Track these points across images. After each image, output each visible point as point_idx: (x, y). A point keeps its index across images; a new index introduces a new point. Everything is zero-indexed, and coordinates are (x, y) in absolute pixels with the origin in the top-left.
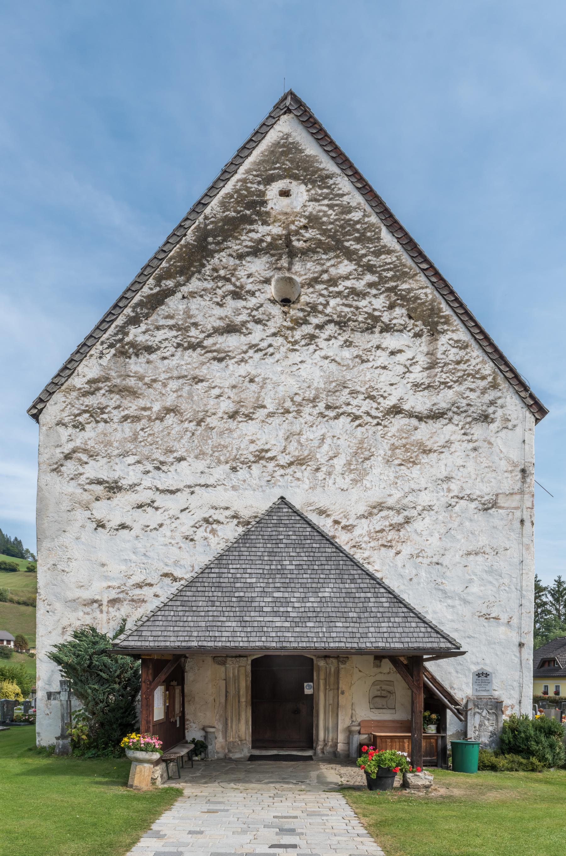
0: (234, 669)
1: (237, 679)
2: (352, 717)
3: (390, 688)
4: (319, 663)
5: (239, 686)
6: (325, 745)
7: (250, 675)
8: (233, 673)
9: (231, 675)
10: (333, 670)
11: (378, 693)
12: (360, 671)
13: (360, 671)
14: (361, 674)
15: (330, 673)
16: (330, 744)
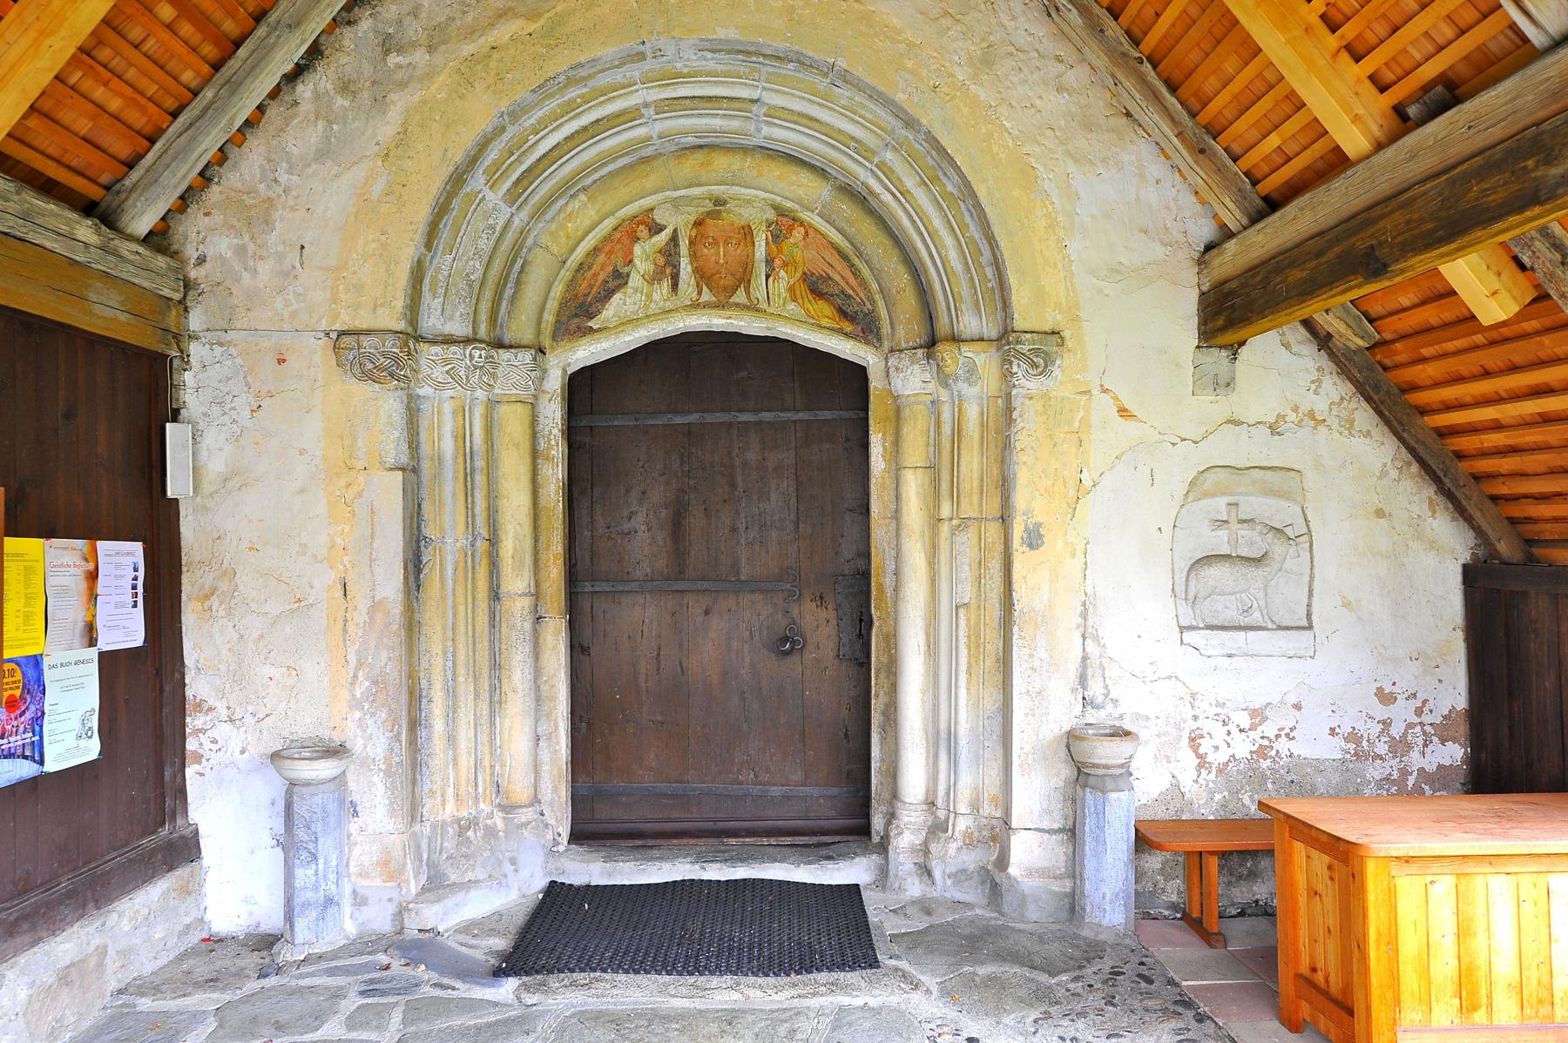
0: (462, 412)
1: (478, 470)
2: (1083, 680)
3: (1282, 512)
4: (898, 383)
6: (938, 829)
7: (557, 449)
8: (461, 437)
9: (448, 446)
10: (972, 412)
11: (1220, 542)
12: (1123, 412)
13: (1123, 412)
14: (1130, 426)
15: (958, 432)
16: (962, 824)
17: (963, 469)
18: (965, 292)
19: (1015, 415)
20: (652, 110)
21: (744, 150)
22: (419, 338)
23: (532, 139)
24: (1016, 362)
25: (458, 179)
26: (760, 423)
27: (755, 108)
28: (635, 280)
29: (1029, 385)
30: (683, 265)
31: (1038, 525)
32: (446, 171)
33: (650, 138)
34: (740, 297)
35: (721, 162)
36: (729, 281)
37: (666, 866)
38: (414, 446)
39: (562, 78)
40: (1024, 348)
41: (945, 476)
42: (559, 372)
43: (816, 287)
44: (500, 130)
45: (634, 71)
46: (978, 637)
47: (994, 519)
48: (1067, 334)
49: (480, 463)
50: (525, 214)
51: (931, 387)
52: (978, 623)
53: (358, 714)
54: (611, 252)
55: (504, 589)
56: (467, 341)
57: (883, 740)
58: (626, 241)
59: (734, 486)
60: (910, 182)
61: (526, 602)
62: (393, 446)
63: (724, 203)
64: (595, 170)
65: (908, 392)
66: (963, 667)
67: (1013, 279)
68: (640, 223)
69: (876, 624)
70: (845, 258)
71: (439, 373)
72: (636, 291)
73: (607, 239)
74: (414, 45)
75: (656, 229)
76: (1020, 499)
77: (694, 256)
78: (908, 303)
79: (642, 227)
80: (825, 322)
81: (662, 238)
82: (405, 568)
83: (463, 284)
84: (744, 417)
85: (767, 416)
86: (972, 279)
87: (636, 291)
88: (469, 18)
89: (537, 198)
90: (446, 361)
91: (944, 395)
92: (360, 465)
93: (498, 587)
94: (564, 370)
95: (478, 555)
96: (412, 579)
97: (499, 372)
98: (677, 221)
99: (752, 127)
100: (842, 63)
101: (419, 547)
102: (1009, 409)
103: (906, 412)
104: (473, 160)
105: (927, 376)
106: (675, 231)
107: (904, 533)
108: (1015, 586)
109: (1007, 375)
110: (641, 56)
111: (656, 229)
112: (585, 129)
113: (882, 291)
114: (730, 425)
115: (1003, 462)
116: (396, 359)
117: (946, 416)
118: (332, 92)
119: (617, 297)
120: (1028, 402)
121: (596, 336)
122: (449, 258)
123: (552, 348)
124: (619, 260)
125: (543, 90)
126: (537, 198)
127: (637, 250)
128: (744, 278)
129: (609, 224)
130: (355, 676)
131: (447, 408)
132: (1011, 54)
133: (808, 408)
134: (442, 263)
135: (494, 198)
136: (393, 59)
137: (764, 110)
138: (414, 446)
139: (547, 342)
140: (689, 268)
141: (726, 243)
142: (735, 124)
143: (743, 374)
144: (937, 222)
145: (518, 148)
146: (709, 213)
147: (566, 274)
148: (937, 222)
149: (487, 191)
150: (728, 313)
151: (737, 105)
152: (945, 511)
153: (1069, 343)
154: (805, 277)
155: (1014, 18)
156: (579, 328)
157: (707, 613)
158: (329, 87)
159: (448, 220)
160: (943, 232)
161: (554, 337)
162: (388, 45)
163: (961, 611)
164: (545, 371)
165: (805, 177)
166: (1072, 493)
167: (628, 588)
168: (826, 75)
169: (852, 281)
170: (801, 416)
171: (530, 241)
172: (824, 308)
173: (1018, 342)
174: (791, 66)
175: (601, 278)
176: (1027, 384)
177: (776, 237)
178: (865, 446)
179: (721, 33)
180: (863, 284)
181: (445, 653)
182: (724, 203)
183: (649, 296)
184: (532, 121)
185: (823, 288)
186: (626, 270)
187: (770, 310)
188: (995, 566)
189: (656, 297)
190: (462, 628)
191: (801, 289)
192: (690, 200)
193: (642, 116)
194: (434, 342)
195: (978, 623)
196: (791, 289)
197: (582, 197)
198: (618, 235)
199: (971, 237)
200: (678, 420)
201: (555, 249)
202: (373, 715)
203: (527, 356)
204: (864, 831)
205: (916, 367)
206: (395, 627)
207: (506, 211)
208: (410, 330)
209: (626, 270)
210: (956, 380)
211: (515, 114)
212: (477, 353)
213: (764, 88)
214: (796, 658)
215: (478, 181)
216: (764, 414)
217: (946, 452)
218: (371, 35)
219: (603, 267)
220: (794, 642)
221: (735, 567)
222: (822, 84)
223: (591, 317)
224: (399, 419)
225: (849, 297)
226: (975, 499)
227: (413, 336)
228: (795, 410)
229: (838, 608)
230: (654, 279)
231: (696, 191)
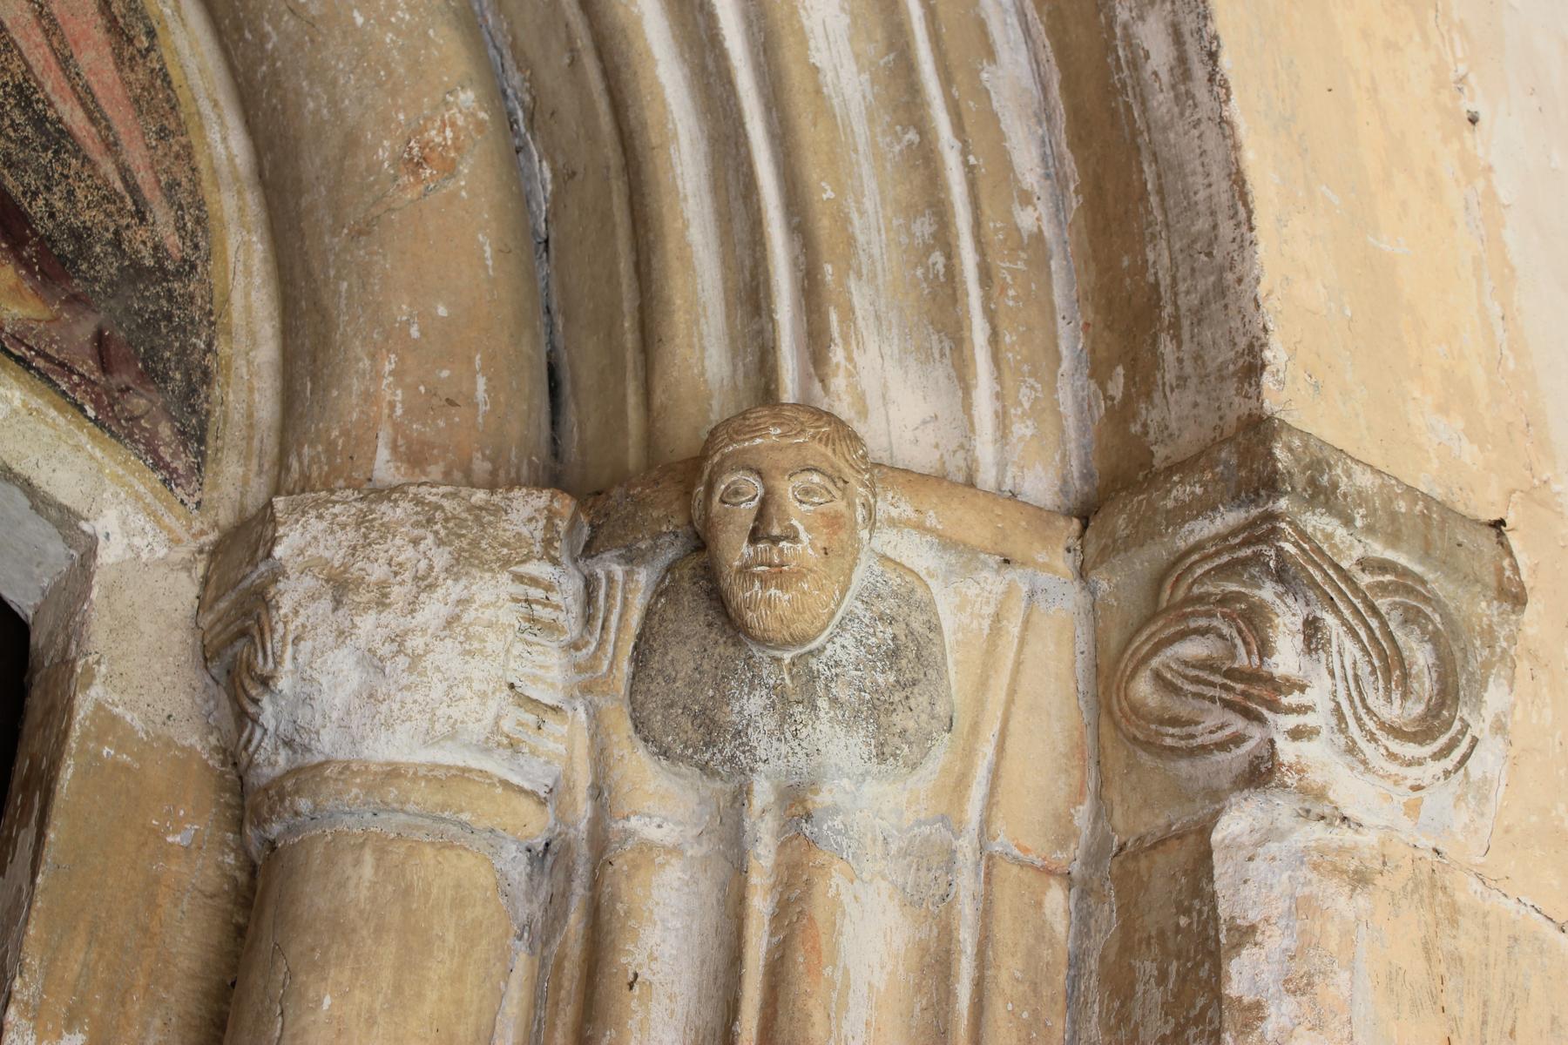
4: (324, 677)
29: (1349, 788)
65: (386, 748)
86: (925, 157)
91: (662, 806)
105: (547, 671)
180: (159, 100)
205: (492, 595)
225: (59, 138)
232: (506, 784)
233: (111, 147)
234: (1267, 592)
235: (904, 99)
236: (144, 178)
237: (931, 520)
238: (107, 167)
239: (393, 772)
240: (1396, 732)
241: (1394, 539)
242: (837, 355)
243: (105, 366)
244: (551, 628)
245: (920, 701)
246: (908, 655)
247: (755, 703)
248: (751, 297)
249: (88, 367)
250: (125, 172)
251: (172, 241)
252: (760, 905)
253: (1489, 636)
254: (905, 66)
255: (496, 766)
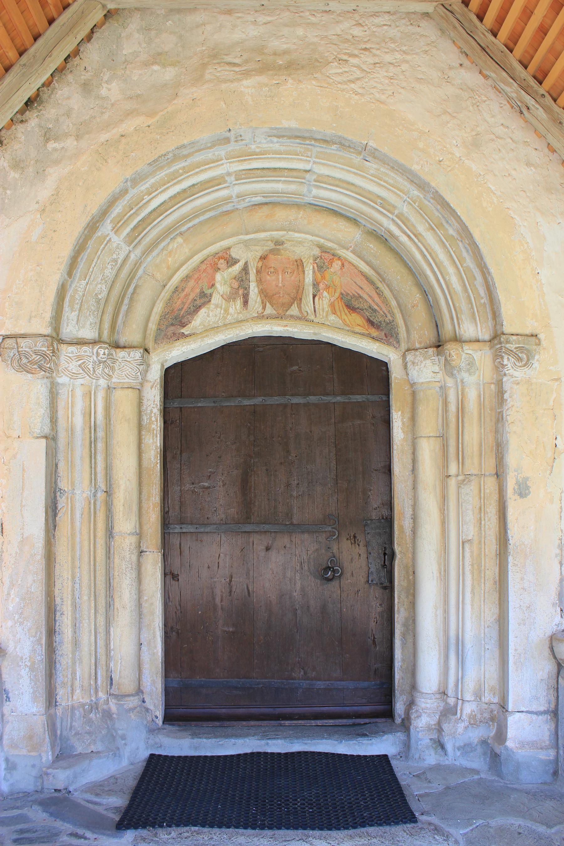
1: (99, 439)
4: (414, 373)
5: (108, 469)
6: (448, 712)
7: (155, 423)
8: (88, 414)
9: (79, 421)
10: (472, 395)
15: (461, 409)
16: (468, 709)
17: (466, 437)
18: (464, 306)
19: (506, 396)
20: (233, 178)
21: (298, 206)
22: (61, 341)
23: (147, 198)
24: (506, 357)
25: (93, 226)
26: (306, 405)
27: (308, 176)
28: (216, 299)
29: (516, 374)
30: (252, 288)
31: (526, 479)
32: (84, 220)
33: (230, 197)
34: (294, 311)
35: (281, 214)
36: (286, 299)
37: (240, 741)
38: (54, 420)
39: (171, 155)
40: (512, 347)
41: (452, 443)
42: (159, 367)
43: (351, 304)
44: (124, 192)
45: (220, 151)
46: (479, 565)
47: (490, 475)
48: (542, 336)
49: (101, 434)
50: (138, 251)
51: (439, 376)
52: (479, 555)
53: (10, 623)
54: (199, 279)
55: (116, 529)
56: (94, 342)
57: (404, 644)
58: (210, 271)
59: (288, 452)
60: (421, 228)
61: (133, 539)
62: (39, 421)
63: (283, 243)
64: (190, 220)
65: (421, 380)
66: (468, 589)
67: (501, 296)
68: (219, 258)
69: (398, 556)
70: (372, 283)
71: (73, 366)
72: (217, 306)
73: (196, 269)
74: (67, 135)
75: (231, 262)
76: (512, 459)
77: (260, 281)
78: (420, 315)
79: (222, 261)
80: (357, 329)
81: (237, 268)
82: (46, 513)
83: (92, 302)
84: (296, 400)
85: (313, 399)
86: (469, 297)
87: (217, 306)
88: (106, 116)
89: (148, 239)
90: (79, 358)
91: (450, 382)
92: (15, 434)
93: (112, 528)
94: (163, 365)
95: (98, 503)
96: (50, 521)
97: (116, 366)
98: (246, 256)
99: (304, 189)
100: (372, 144)
101: (55, 497)
102: (500, 393)
103: (420, 395)
104: (104, 213)
105: (436, 368)
106: (246, 263)
107: (420, 487)
108: (510, 525)
109: (499, 368)
110: (227, 140)
111: (231, 262)
112: (184, 191)
113: (399, 306)
114: (285, 406)
115: (497, 431)
116: (44, 355)
117: (452, 398)
118: (7, 169)
119: (203, 311)
120: (515, 387)
121: (188, 339)
122: (84, 283)
123: (155, 349)
124: (204, 284)
125: (156, 164)
126: (148, 239)
127: (218, 277)
128: (297, 298)
129: (197, 258)
130: (9, 594)
131: (79, 392)
132: (493, 140)
133: (343, 393)
134: (78, 286)
135: (117, 240)
136: (52, 145)
137: (315, 177)
138: (54, 420)
139: (150, 345)
140: (256, 290)
141: (284, 272)
142: (293, 187)
143: (295, 368)
144: (442, 256)
145: (137, 204)
146: (271, 251)
147: (165, 294)
148: (442, 256)
149: (112, 235)
150: (285, 322)
151: (295, 174)
152: (453, 469)
153: (544, 343)
154: (342, 296)
155: (493, 116)
156: (174, 334)
157: (268, 549)
158: (6, 165)
159: (85, 256)
160: (447, 263)
161: (156, 340)
162: (48, 136)
163: (467, 546)
164: (148, 366)
165: (342, 225)
166: (550, 454)
167: (208, 529)
168: (360, 153)
169: (377, 299)
170: (339, 399)
171: (140, 272)
172: (357, 319)
173: (508, 342)
174: (334, 147)
175: (191, 297)
176: (515, 373)
177: (320, 268)
178: (387, 422)
179: (285, 124)
180: (385, 301)
181: (73, 577)
182: (283, 243)
183: (226, 311)
184: (147, 185)
185: (356, 304)
186: (210, 291)
187: (316, 320)
188: (492, 511)
189: (232, 310)
190: (86, 559)
191: (340, 305)
192: (257, 242)
193: (225, 182)
194: (71, 344)
195: (479, 555)
196: (332, 305)
197: (180, 240)
198: (204, 267)
199: (468, 267)
200: (246, 402)
201: (158, 276)
202: (21, 624)
203: (137, 354)
204: (389, 714)
205: (428, 362)
206: (39, 557)
207: (126, 249)
208: (54, 335)
209: (210, 291)
210: (460, 370)
211: (135, 181)
212: (101, 352)
213: (314, 162)
214: (335, 583)
215: (106, 228)
216: (311, 397)
217: (453, 425)
218: (37, 129)
219: (192, 289)
220: (334, 571)
221: (289, 514)
222: (357, 159)
223: (183, 325)
224: (44, 401)
225: (375, 311)
226: (476, 460)
227: (56, 339)
228: (334, 394)
229: (367, 545)
230: (230, 298)
231: (262, 235)
232: (435, 381)
233: (381, 309)
234: (503, 354)
235: (466, 290)
236: (385, 311)
237: (471, 348)
238: (381, 312)
239: (422, 383)
240: (520, 367)
241: (519, 344)
242: (461, 326)
243: (386, 337)
244: (436, 364)
245: (473, 368)
246: (471, 364)
247: (456, 372)
248: (452, 318)
249: (384, 338)
250: (383, 312)
251: (391, 318)
252: (460, 393)
253: (535, 350)
254: (465, 285)
255: (433, 380)
